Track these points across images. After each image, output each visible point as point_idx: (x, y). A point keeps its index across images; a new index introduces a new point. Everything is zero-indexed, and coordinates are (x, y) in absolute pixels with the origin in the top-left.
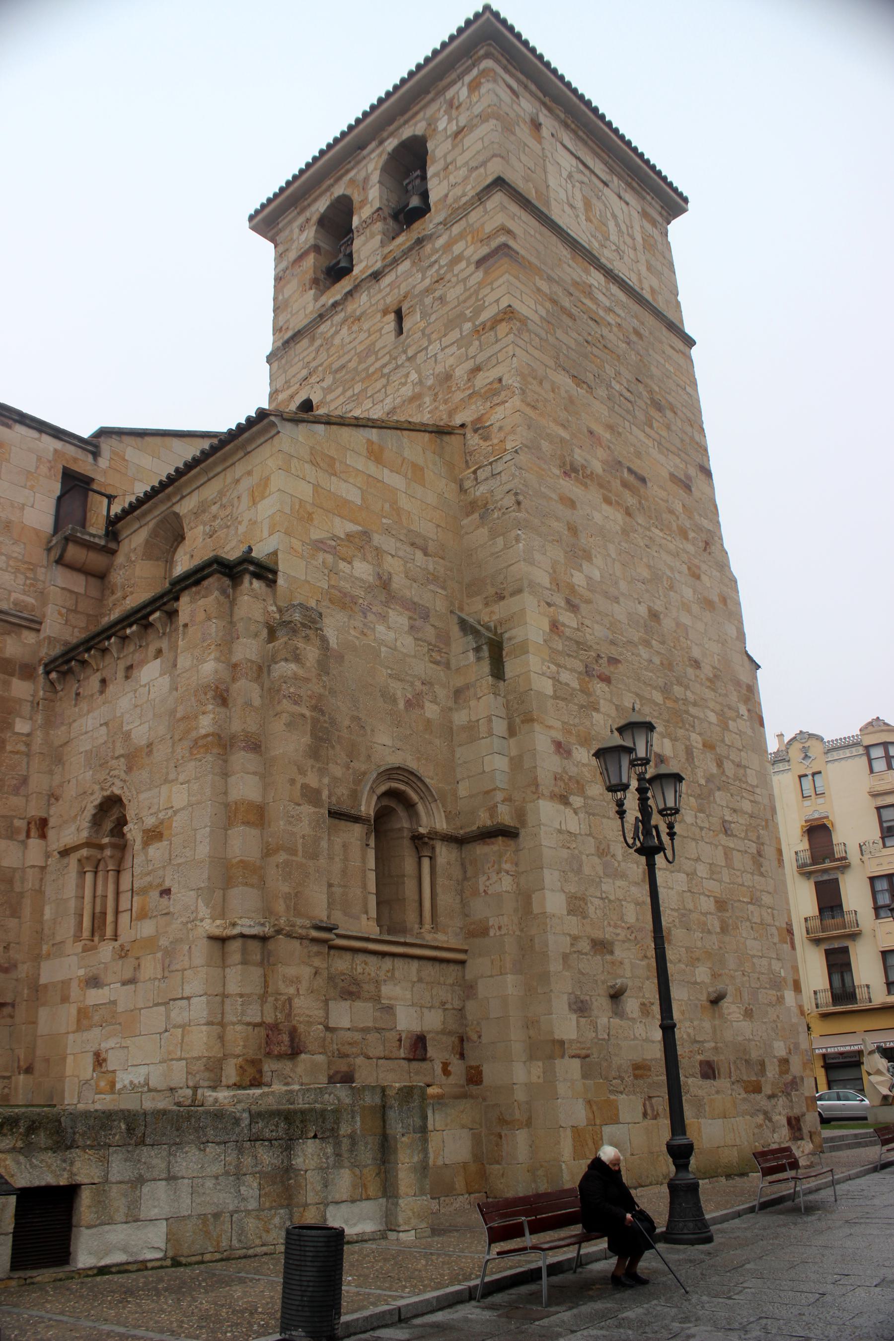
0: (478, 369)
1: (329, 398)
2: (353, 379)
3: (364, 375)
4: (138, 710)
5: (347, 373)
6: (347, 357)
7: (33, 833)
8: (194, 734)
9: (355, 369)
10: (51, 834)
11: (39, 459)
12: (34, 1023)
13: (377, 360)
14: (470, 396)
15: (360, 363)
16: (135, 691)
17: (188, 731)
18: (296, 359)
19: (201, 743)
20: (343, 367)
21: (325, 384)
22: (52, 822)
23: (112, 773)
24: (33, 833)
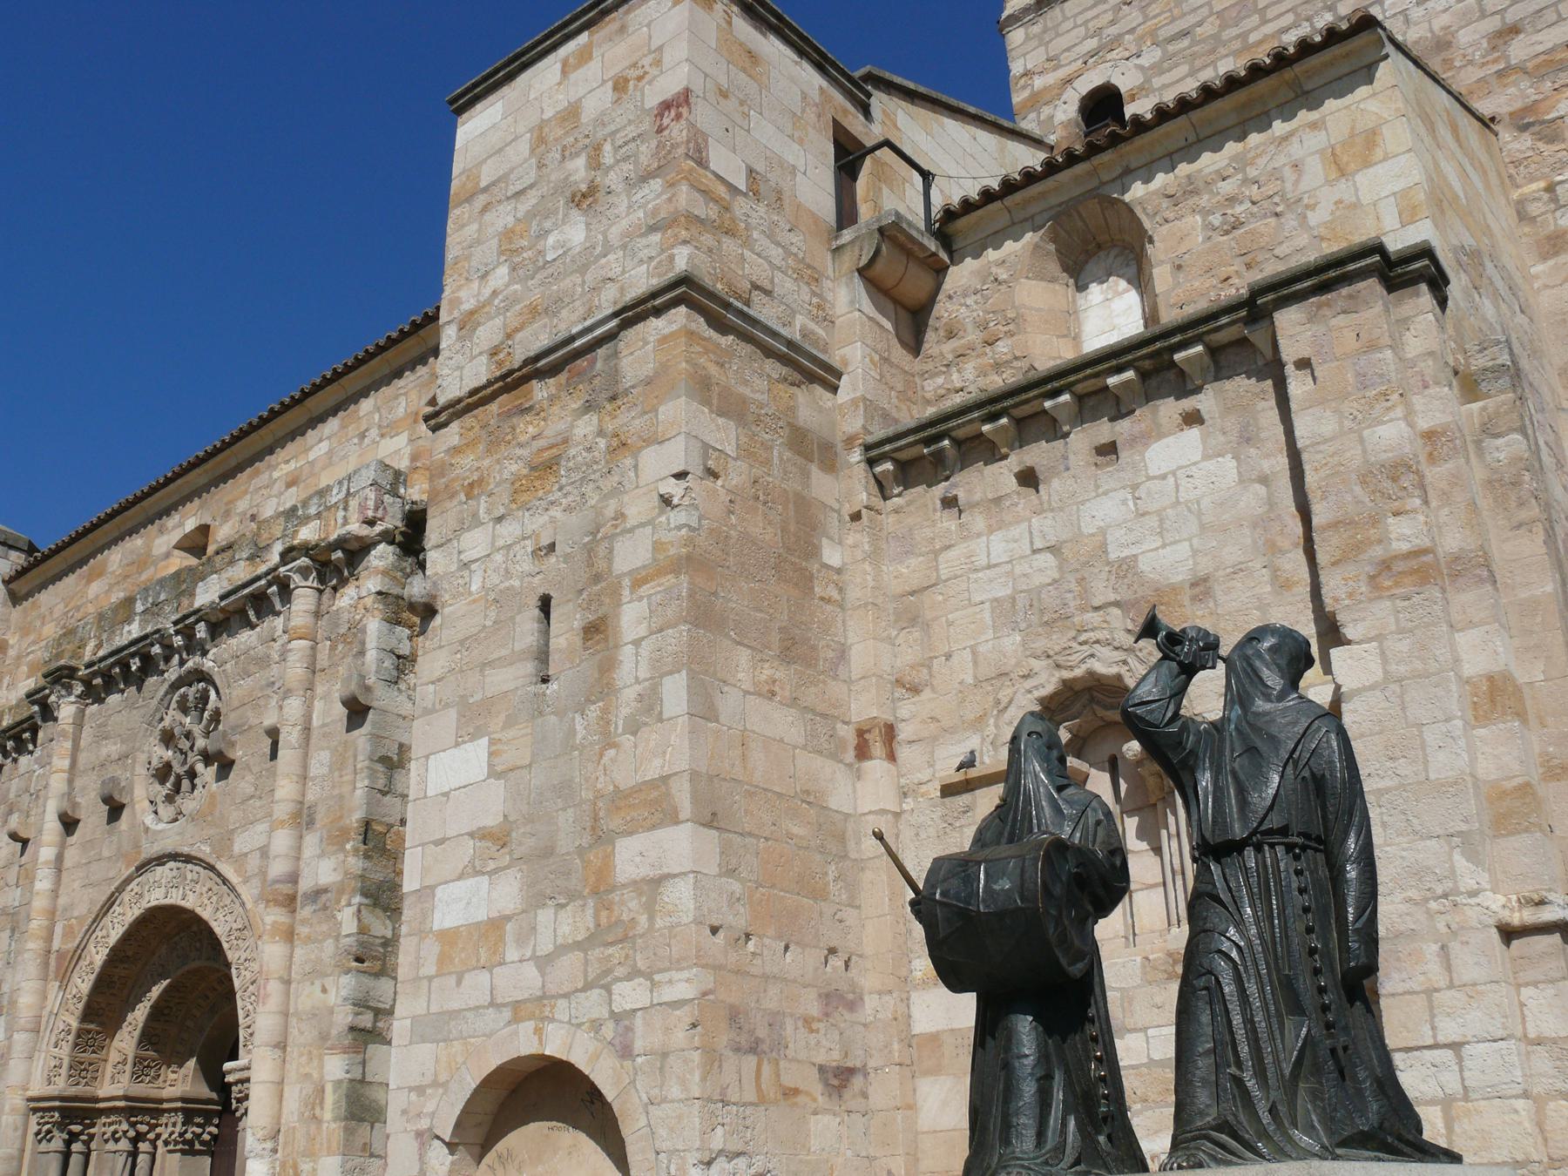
0: (1514, 30)
1: (1157, 82)
2: (1212, 51)
3: (1237, 45)
4: (1153, 521)
5: (1194, 43)
6: (1192, 19)
7: (878, 748)
8: (1378, 552)
9: (1216, 37)
10: (903, 753)
11: (804, 96)
12: (910, 1107)
13: (1264, 22)
14: (1500, 74)
15: (1223, 27)
16: (1135, 487)
17: (1359, 547)
18: (1069, 24)
19: (1400, 566)
20: (1185, 33)
21: (1145, 61)
22: (905, 732)
23: (1083, 638)
24: (878, 748)
